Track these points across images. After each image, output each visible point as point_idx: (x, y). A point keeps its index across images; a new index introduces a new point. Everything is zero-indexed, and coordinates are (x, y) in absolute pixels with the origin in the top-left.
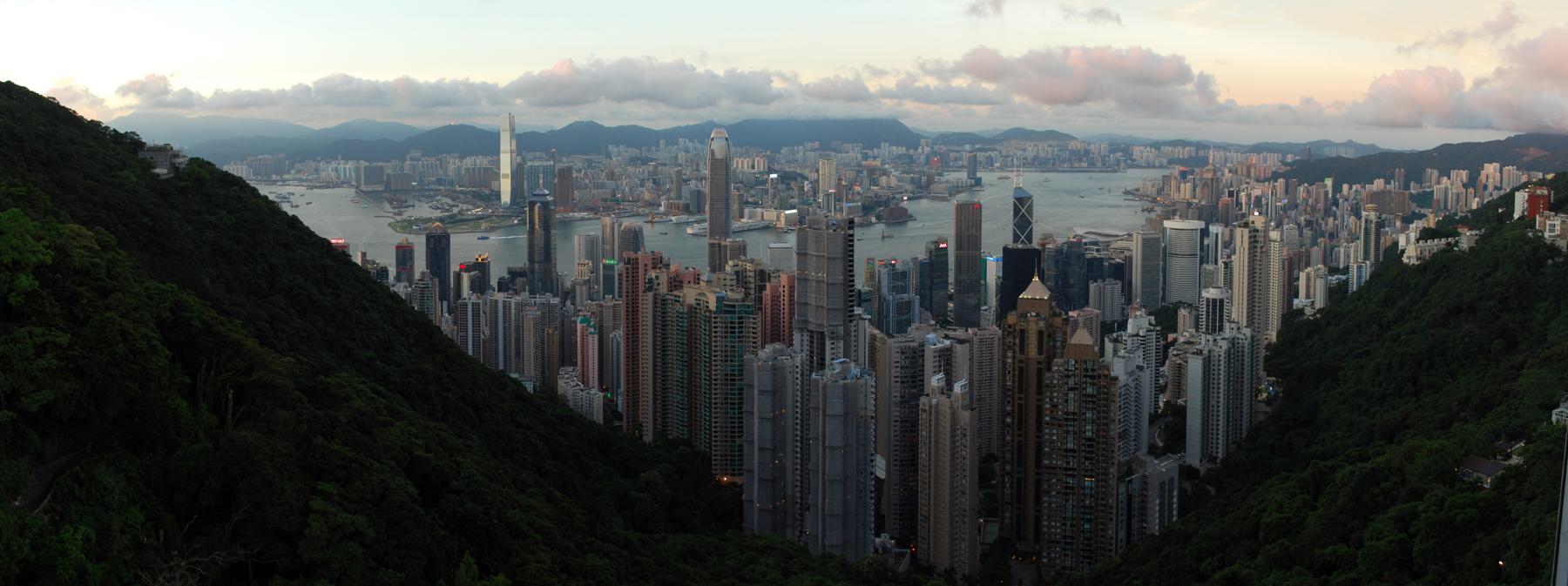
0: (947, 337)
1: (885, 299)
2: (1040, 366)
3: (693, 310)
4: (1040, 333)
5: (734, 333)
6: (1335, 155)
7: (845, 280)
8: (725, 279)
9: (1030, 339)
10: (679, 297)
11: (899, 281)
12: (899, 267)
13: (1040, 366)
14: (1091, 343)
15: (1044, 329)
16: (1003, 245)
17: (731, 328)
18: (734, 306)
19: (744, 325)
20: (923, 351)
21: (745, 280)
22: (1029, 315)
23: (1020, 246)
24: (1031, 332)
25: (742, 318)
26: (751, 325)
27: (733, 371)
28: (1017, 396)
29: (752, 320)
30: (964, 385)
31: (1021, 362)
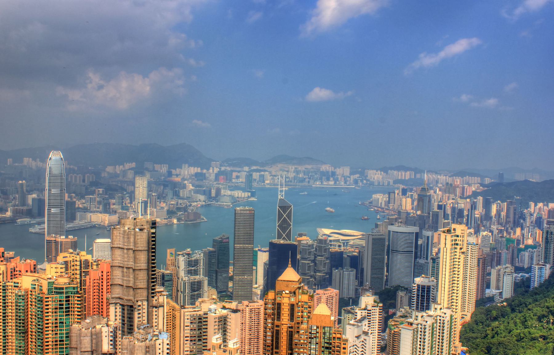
0: (224, 308)
1: (182, 279)
2: (291, 330)
3: (30, 293)
4: (292, 307)
6: (523, 179)
7: (148, 266)
8: (56, 268)
10: (18, 283)
11: (193, 267)
13: (291, 330)
14: (329, 314)
15: (295, 303)
16: (270, 241)
17: (60, 305)
18: (62, 288)
19: (70, 302)
21: (72, 268)
22: (284, 292)
23: (282, 242)
24: (285, 304)
25: (68, 297)
26: (76, 302)
27: (62, 337)
28: (275, 350)
29: (76, 298)
30: (236, 343)
31: (278, 326)
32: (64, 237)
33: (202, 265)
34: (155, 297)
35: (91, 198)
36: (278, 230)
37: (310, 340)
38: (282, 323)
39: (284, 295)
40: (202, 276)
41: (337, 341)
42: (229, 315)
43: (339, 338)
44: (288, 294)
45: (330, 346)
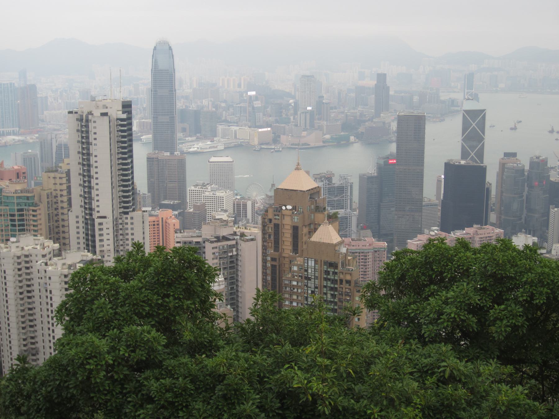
4: (295, 229)
5: (14, 226)
8: (54, 178)
9: (286, 235)
12: (336, 181)
15: (300, 225)
16: (446, 161)
17: (12, 220)
19: (25, 217)
20: (204, 247)
22: (284, 208)
23: (463, 162)
25: (22, 210)
29: (31, 212)
32: (168, 154)
33: (349, 194)
34: (129, 213)
35: (241, 107)
36: (463, 147)
37: (306, 281)
38: (284, 255)
39: (284, 213)
40: (349, 210)
41: (344, 285)
42: (239, 245)
43: (348, 282)
44: (290, 210)
45: (336, 293)
